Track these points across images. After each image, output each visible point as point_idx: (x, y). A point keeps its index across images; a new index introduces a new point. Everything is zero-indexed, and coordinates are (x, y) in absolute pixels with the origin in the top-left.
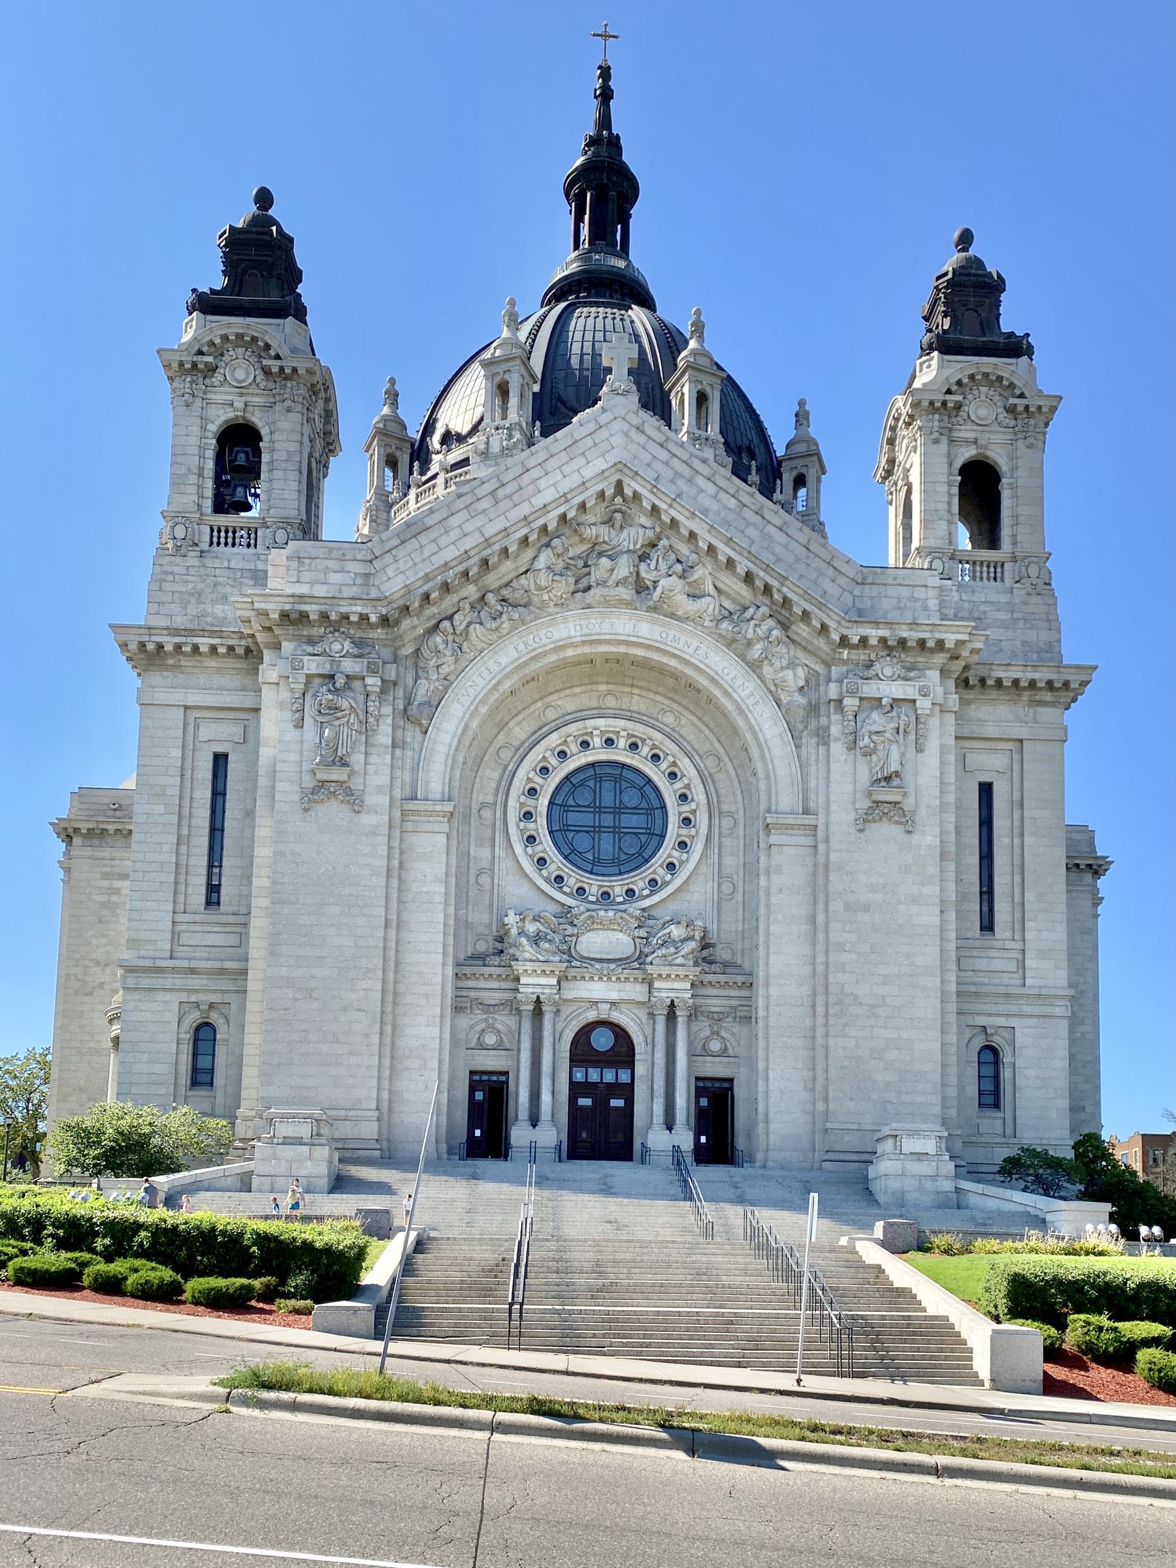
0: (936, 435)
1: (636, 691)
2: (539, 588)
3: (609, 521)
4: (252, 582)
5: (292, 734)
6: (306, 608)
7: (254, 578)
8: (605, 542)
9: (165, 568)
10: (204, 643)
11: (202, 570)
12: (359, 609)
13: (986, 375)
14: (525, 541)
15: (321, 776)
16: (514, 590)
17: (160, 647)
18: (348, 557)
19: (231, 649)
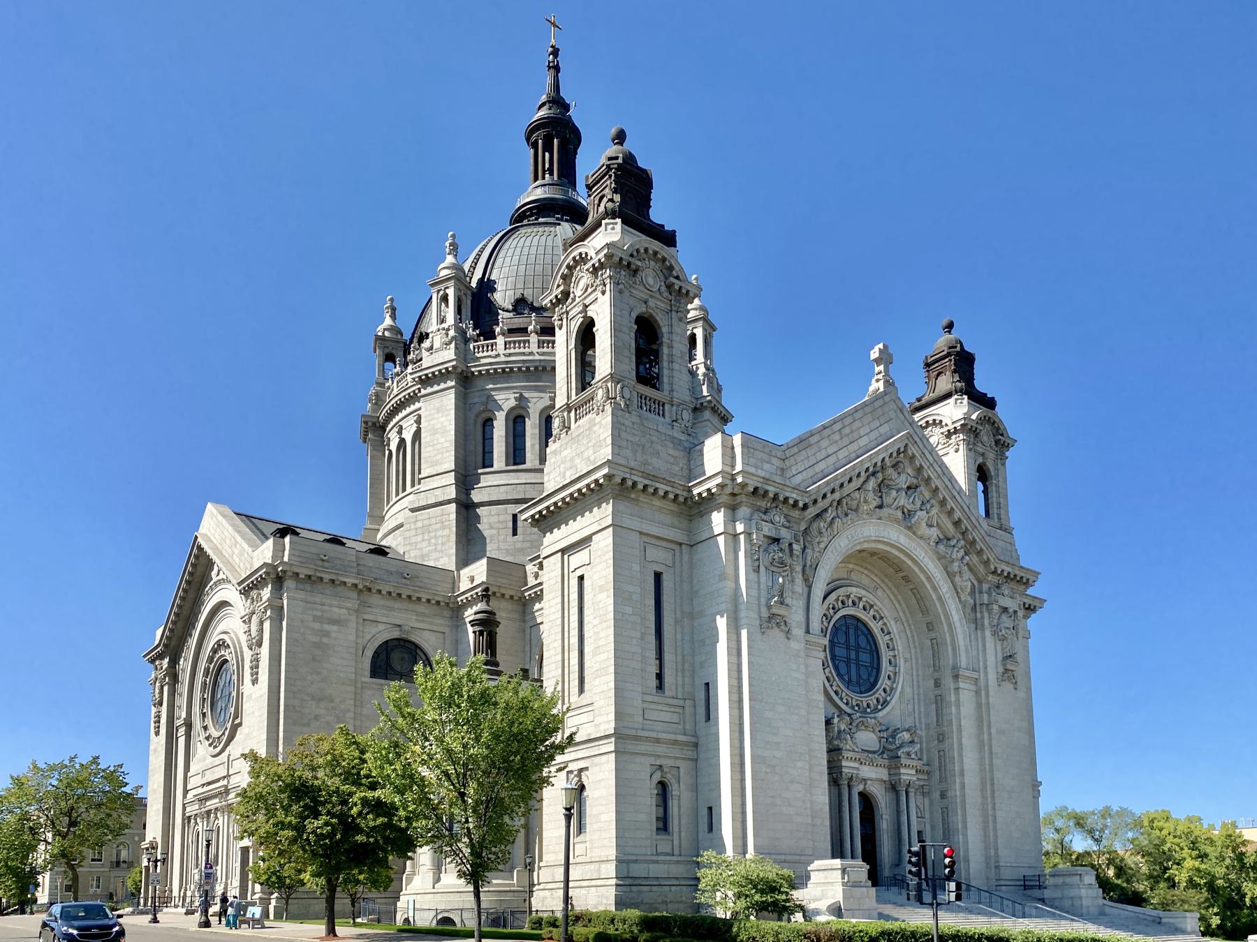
0: (971, 446)
1: (866, 572)
2: (866, 501)
3: (895, 466)
4: (671, 445)
5: (753, 576)
6: (771, 489)
7: (672, 442)
8: (891, 480)
9: (619, 419)
10: (663, 488)
11: (642, 427)
12: (795, 496)
13: (990, 418)
14: (867, 469)
15: (774, 611)
16: (852, 499)
17: (635, 484)
18: (773, 454)
19: (676, 496)
